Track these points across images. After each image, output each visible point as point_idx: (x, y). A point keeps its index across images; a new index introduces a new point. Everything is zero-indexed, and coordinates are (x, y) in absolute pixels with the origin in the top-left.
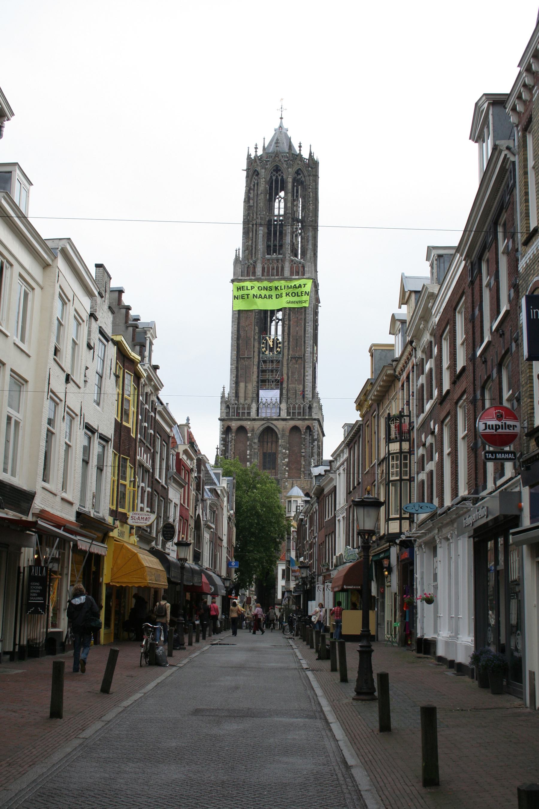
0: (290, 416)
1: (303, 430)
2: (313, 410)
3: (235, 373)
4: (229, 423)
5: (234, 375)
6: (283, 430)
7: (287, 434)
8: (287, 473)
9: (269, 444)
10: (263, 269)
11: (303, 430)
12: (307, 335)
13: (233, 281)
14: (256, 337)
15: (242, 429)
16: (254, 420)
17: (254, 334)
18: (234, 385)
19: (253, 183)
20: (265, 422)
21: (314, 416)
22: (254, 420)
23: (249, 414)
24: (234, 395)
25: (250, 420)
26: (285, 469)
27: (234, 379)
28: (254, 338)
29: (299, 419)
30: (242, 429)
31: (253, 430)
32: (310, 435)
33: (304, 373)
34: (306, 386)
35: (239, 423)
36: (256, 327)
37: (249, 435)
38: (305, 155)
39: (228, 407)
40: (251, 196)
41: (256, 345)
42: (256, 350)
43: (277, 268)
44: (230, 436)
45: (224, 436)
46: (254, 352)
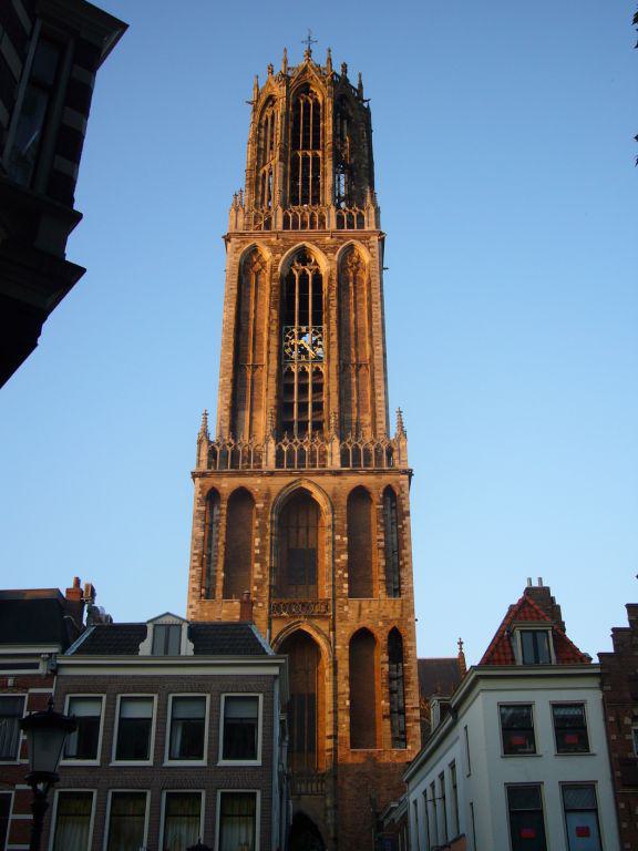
0: (348, 466)
1: (377, 495)
2: (395, 454)
3: (230, 391)
4: (214, 482)
5: (228, 394)
6: (335, 495)
7: (344, 502)
8: (346, 586)
9: (302, 531)
10: (286, 219)
11: (377, 495)
12: (374, 324)
13: (227, 239)
14: (274, 328)
15: (242, 496)
16: (272, 474)
17: (270, 323)
18: (227, 413)
19: (264, 119)
20: (293, 479)
21: (401, 467)
22: (272, 474)
23: (258, 459)
24: (226, 431)
25: (262, 474)
26: (341, 576)
27: (228, 402)
28: (269, 328)
29: (369, 473)
30: (242, 496)
31: (268, 496)
32: (392, 508)
33: (373, 390)
34: (378, 413)
35: (238, 482)
36: (273, 311)
37: (260, 505)
38: (354, 83)
39: (212, 453)
40: (263, 135)
41: (274, 341)
42: (274, 349)
43: (312, 216)
44: (216, 512)
45: (203, 509)
46: (269, 352)
